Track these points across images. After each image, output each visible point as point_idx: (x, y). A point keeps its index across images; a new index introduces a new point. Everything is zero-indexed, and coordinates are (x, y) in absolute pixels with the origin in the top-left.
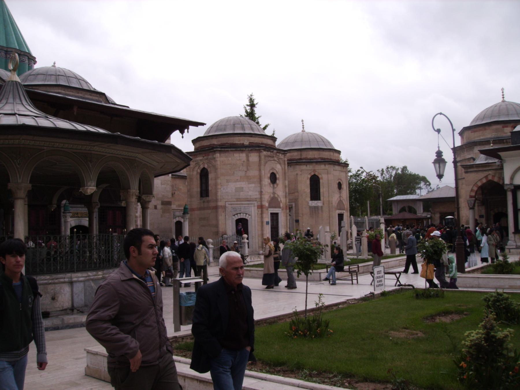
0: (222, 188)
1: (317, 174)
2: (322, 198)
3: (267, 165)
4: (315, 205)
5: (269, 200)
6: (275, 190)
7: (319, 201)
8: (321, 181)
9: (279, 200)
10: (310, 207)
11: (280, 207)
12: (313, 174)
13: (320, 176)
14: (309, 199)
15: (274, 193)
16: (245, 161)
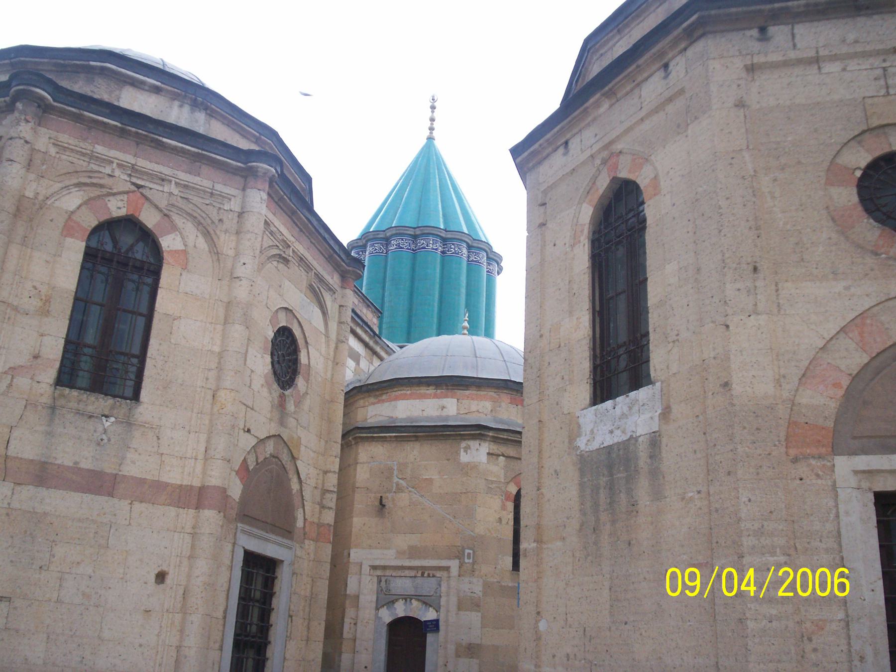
1: (623, 174)
4: (609, 441)
12: (603, 183)
13: (643, 180)
14: (584, 390)
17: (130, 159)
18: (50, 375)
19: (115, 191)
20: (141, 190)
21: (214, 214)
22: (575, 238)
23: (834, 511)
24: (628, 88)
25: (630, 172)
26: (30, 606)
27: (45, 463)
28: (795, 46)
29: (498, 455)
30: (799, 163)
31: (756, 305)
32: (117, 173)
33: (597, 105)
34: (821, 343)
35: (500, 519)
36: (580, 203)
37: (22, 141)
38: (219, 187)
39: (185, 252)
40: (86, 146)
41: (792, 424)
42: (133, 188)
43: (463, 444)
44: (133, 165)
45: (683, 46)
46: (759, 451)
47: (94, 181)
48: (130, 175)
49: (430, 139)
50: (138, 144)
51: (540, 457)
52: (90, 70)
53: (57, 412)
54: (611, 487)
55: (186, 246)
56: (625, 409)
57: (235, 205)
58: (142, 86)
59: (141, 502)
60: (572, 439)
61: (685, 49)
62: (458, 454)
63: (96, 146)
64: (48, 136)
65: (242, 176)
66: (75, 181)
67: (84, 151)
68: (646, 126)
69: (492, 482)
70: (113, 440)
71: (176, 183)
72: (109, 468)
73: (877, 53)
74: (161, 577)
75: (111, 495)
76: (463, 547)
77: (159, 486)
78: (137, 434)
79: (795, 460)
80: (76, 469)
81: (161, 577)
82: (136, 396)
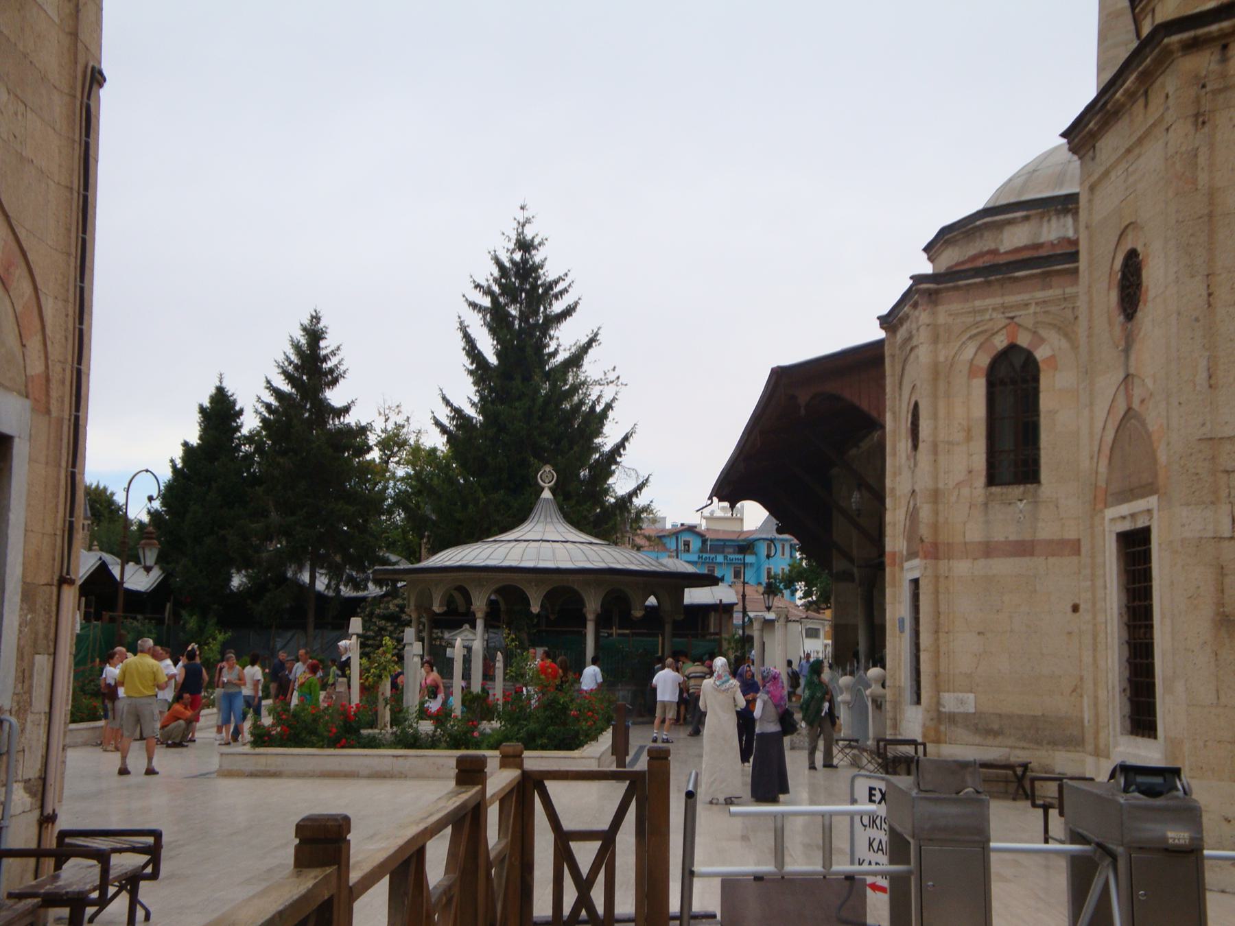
17: (998, 301)
18: (981, 480)
19: (996, 330)
32: (994, 315)
39: (1053, 356)
40: (968, 306)
42: (1008, 321)
47: (980, 329)
48: (1003, 313)
52: (979, 228)
55: (1053, 350)
67: (968, 310)
71: (1037, 304)
72: (1028, 537)
74: (1075, 609)
81: (1075, 609)
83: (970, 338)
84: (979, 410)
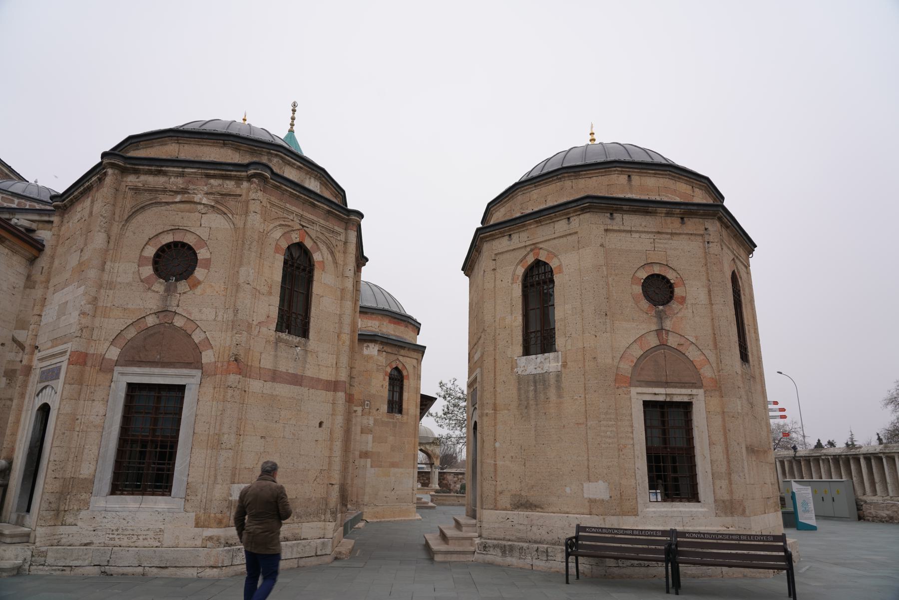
0: (43, 314)
1: (542, 258)
2: (560, 341)
3: (140, 218)
4: (534, 372)
5: (132, 333)
6: (174, 303)
7: (551, 355)
8: (557, 278)
9: (197, 337)
10: (520, 379)
11: (195, 363)
12: (530, 260)
13: (554, 264)
14: (519, 349)
15: (163, 311)
16: (87, 219)
19: (294, 229)
20: (304, 228)
21: (334, 242)
22: (513, 280)
23: (630, 407)
24: (548, 222)
25: (546, 259)
26: (273, 440)
27: (275, 370)
28: (623, 224)
29: (383, 351)
30: (622, 274)
31: (606, 329)
33: (530, 224)
34: (628, 345)
35: (382, 385)
36: (517, 265)
37: (259, 202)
38: (336, 228)
41: (617, 375)
43: (365, 345)
44: (302, 215)
45: (578, 213)
46: (606, 384)
47: (286, 223)
48: (300, 220)
49: (291, 131)
50: (303, 203)
51: (495, 375)
53: (278, 345)
54: (535, 391)
55: (323, 259)
56: (542, 360)
57: (342, 238)
58: (294, 166)
59: (312, 388)
60: (512, 368)
61: (579, 215)
62: (363, 350)
63: (287, 204)
64: (266, 198)
65: (345, 222)
66: (278, 223)
67: (282, 207)
68: (556, 241)
69: (380, 366)
70: (300, 359)
71: (319, 225)
72: (299, 372)
73: (652, 232)
74: (321, 424)
75: (301, 385)
76: (364, 400)
77: (319, 380)
78: (309, 355)
79: (618, 388)
80: (287, 374)
81: (321, 424)
82: (305, 333)
83: (280, 225)
84: (278, 276)
